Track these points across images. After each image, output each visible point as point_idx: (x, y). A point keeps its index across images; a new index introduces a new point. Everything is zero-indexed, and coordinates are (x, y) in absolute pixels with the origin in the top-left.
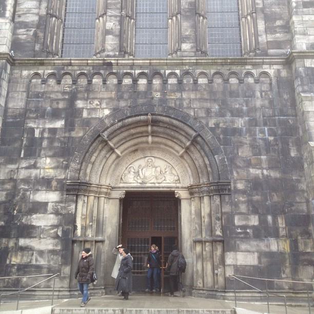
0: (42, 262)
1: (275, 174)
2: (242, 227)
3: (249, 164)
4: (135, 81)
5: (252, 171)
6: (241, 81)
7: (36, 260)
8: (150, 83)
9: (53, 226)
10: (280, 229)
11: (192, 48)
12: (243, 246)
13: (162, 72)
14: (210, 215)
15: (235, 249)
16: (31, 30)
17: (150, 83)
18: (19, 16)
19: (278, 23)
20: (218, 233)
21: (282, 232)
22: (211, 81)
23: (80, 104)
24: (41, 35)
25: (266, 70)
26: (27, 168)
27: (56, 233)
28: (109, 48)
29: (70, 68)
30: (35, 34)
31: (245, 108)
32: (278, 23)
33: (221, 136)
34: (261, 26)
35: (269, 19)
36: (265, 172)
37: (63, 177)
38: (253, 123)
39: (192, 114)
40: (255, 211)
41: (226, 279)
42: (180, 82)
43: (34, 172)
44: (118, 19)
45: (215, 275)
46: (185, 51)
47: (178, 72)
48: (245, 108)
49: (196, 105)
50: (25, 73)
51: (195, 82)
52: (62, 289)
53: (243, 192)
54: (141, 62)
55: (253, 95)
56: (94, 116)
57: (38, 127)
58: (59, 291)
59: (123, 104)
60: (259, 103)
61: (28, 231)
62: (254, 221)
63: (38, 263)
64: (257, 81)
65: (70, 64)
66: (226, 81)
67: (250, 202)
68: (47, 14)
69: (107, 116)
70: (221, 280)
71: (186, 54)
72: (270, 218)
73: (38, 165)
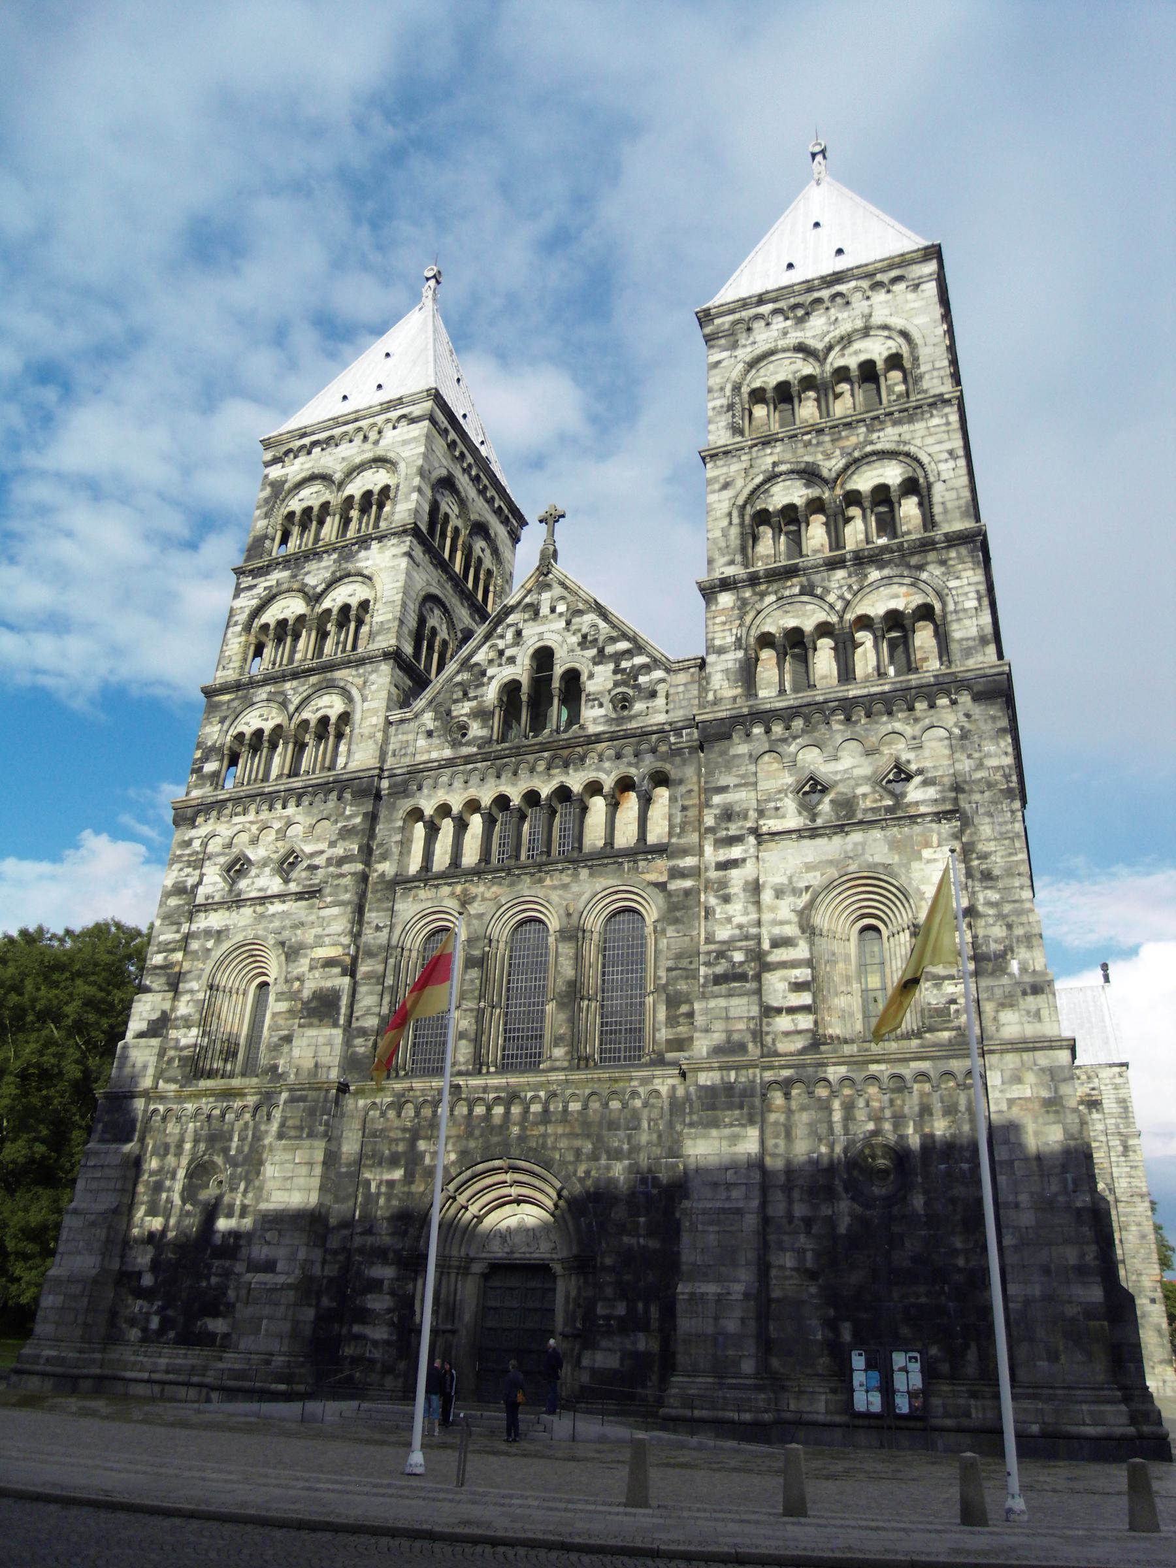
11: (567, 1053)
28: (462, 1059)
71: (558, 1064)
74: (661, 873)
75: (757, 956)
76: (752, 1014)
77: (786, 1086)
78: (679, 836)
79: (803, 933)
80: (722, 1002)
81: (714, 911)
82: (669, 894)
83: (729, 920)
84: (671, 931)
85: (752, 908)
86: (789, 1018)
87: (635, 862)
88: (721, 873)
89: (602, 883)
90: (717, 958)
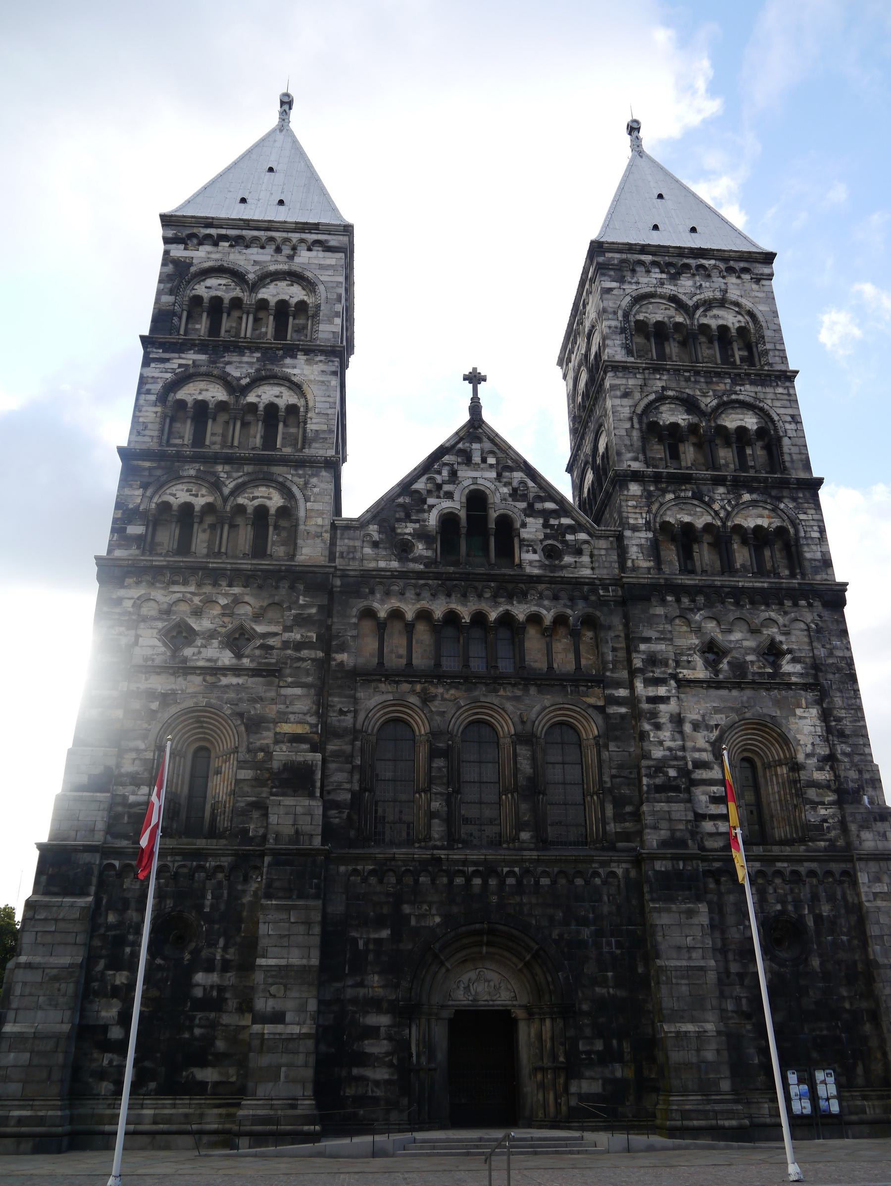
0: (379, 1093)
1: (621, 993)
2: (586, 1052)
5: (597, 989)
6: (587, 883)
7: (372, 1091)
8: (485, 883)
9: (387, 1054)
10: (625, 1054)
11: (532, 837)
12: (588, 1073)
13: (499, 869)
14: (552, 1039)
15: (579, 1076)
16: (344, 812)
17: (485, 883)
18: (329, 792)
19: (628, 809)
20: (562, 1059)
21: (627, 1057)
22: (554, 882)
24: (355, 817)
25: (614, 870)
26: (353, 986)
27: (391, 1061)
28: (436, 836)
29: (393, 863)
30: (349, 816)
31: (591, 916)
32: (628, 809)
33: (566, 950)
34: (609, 811)
35: (619, 803)
36: (611, 991)
37: (394, 997)
39: (534, 922)
41: (570, 1108)
42: (519, 883)
43: (362, 991)
44: (445, 797)
45: (557, 1105)
46: (523, 842)
47: (517, 869)
48: (591, 916)
51: (537, 883)
52: (402, 1122)
54: (475, 857)
56: (423, 924)
57: (362, 937)
58: (399, 1124)
59: (455, 909)
60: (606, 910)
61: (364, 1059)
62: (599, 1046)
63: (374, 1094)
64: (605, 883)
66: (571, 882)
68: (360, 789)
69: (438, 924)
70: (564, 1109)
71: (525, 845)
72: (615, 1042)
73: (366, 982)
74: (599, 698)
75: (684, 773)
76: (689, 818)
78: (612, 671)
79: (716, 760)
80: (664, 806)
81: (649, 735)
82: (607, 717)
83: (661, 743)
84: (612, 747)
85: (677, 736)
86: (712, 823)
87: (577, 686)
88: (652, 706)
89: (548, 700)
90: (655, 772)
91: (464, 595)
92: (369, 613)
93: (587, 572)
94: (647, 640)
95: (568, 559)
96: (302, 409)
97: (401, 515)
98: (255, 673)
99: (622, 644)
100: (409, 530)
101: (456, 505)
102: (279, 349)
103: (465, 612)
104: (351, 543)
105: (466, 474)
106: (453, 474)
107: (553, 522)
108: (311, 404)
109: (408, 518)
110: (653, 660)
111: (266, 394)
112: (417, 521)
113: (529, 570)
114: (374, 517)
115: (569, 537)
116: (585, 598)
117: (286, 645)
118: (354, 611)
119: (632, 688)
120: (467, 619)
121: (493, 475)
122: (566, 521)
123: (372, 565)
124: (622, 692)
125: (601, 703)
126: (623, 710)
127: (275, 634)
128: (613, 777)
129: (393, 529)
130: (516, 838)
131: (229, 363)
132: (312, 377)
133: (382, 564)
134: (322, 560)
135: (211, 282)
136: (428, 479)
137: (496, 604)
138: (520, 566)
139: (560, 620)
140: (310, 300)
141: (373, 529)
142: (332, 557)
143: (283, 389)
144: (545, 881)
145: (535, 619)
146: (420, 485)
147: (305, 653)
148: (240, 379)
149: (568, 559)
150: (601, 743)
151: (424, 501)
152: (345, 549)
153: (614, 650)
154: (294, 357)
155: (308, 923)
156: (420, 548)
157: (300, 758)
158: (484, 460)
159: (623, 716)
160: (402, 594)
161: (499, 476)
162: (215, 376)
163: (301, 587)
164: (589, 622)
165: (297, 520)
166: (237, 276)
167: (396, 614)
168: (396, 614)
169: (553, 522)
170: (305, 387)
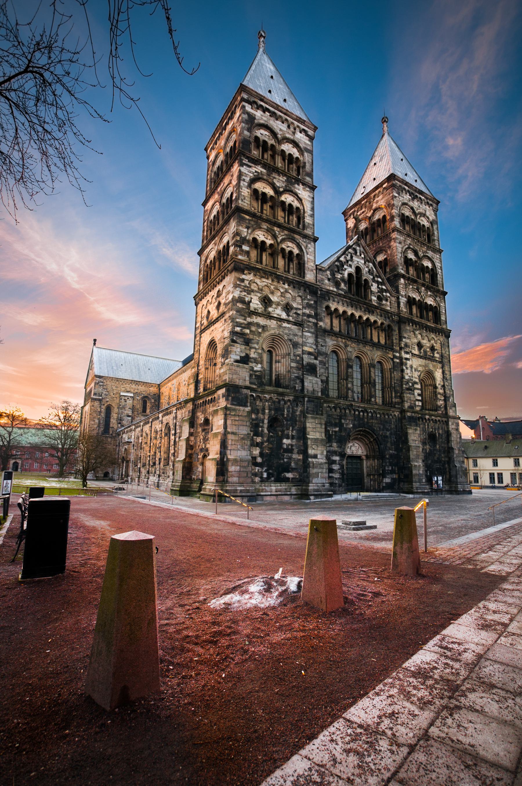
1: (396, 453)
3: (390, 449)
4: (359, 413)
8: (363, 415)
12: (388, 476)
15: (386, 477)
17: (363, 415)
19: (399, 394)
22: (381, 416)
23: (343, 421)
34: (393, 395)
35: (396, 392)
38: (391, 434)
40: (390, 465)
49: (377, 425)
50: (325, 405)
53: (388, 459)
55: (391, 423)
62: (390, 469)
64: (392, 418)
65: (340, 403)
66: (385, 416)
67: (389, 462)
70: (381, 487)
77: (419, 418)
82: (394, 362)
83: (407, 374)
91: (356, 308)
92: (328, 308)
93: (389, 308)
94: (405, 338)
95: (384, 302)
96: (302, 211)
97: (336, 269)
98: (295, 324)
99: (398, 338)
100: (339, 277)
101: (352, 270)
102: (293, 179)
103: (357, 314)
104: (322, 277)
105: (355, 258)
106: (352, 257)
107: (380, 286)
108: (306, 210)
109: (338, 271)
110: (406, 345)
111: (287, 198)
112: (341, 274)
113: (374, 303)
114: (329, 268)
115: (384, 294)
116: (389, 318)
117: (304, 314)
118: (324, 307)
119: (400, 353)
120: (357, 318)
121: (363, 262)
122: (384, 287)
123: (328, 288)
124: (398, 355)
125: (392, 357)
126: (398, 361)
127: (300, 309)
128: (395, 383)
129: (334, 275)
130: (370, 400)
131: (275, 178)
132: (305, 197)
133: (331, 289)
134: (313, 281)
135: (262, 131)
136: (345, 257)
137: (365, 314)
138: (371, 300)
139: (382, 324)
140: (301, 158)
141: (328, 272)
142: (316, 282)
143: (294, 199)
144: (378, 416)
145: (375, 322)
146: (342, 259)
147: (311, 319)
148: (279, 188)
149: (384, 302)
150: (391, 371)
151: (343, 267)
152: (320, 279)
153: (396, 339)
154: (299, 185)
155: (321, 424)
156: (343, 285)
157: (312, 362)
158: (361, 255)
159: (398, 363)
160: (339, 302)
161: (365, 263)
162: (268, 182)
163: (308, 291)
164: (389, 326)
165: (304, 261)
166: (274, 134)
167: (336, 310)
168: (336, 310)
169: (380, 286)
170: (303, 201)
